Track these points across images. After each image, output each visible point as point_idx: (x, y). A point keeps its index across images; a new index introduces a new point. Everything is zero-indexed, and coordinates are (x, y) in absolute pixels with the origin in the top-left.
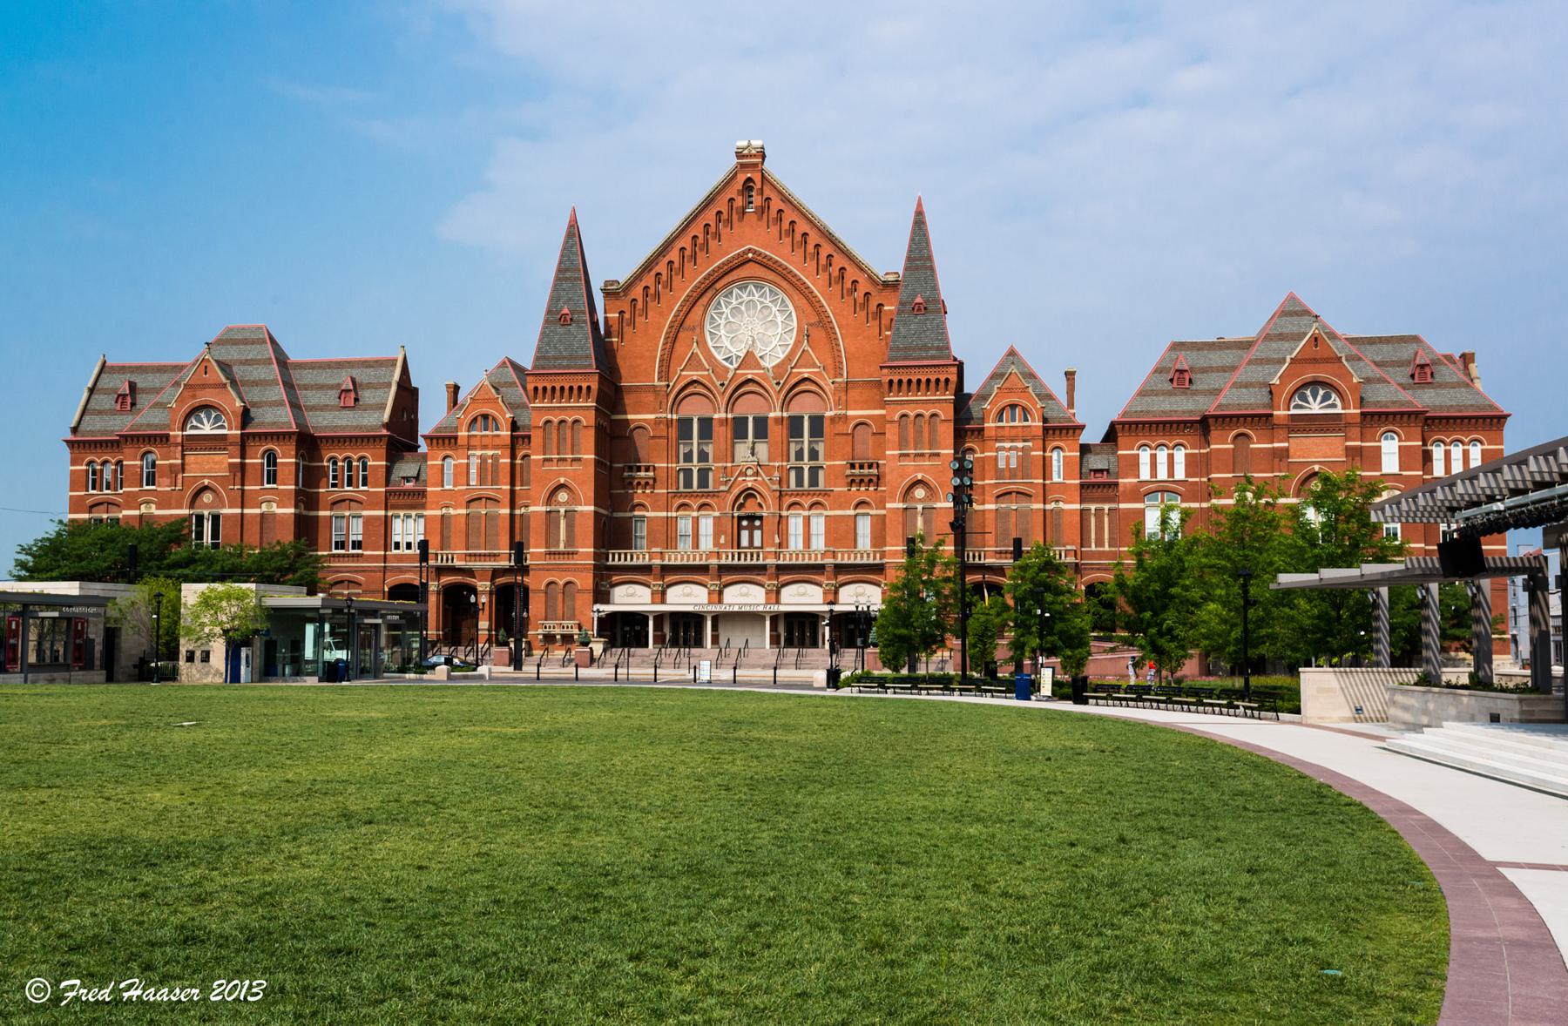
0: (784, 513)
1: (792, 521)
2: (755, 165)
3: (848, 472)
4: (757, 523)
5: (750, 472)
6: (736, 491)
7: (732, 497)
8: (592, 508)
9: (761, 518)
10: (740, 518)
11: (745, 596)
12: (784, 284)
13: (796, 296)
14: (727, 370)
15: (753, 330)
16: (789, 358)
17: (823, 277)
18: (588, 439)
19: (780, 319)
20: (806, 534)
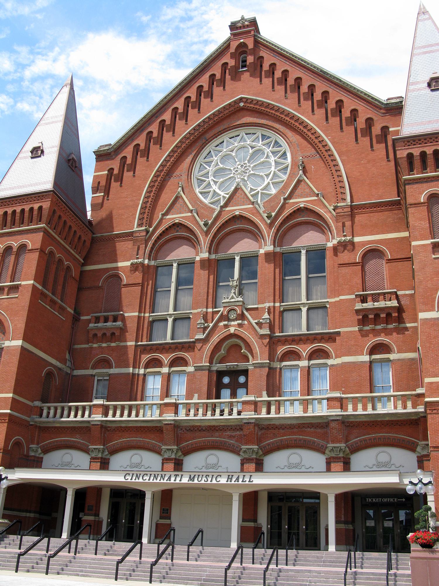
0: (277, 365)
1: (287, 375)
2: (249, 32)
3: (359, 306)
4: (242, 379)
5: (232, 316)
6: (215, 339)
7: (209, 347)
8: (19, 343)
9: (245, 372)
10: (221, 374)
11: (218, 471)
12: (277, 126)
13: (289, 133)
14: (213, 210)
15: (247, 170)
16: (281, 192)
17: (320, 113)
18: (30, 263)
19: (272, 159)
20: (308, 395)
